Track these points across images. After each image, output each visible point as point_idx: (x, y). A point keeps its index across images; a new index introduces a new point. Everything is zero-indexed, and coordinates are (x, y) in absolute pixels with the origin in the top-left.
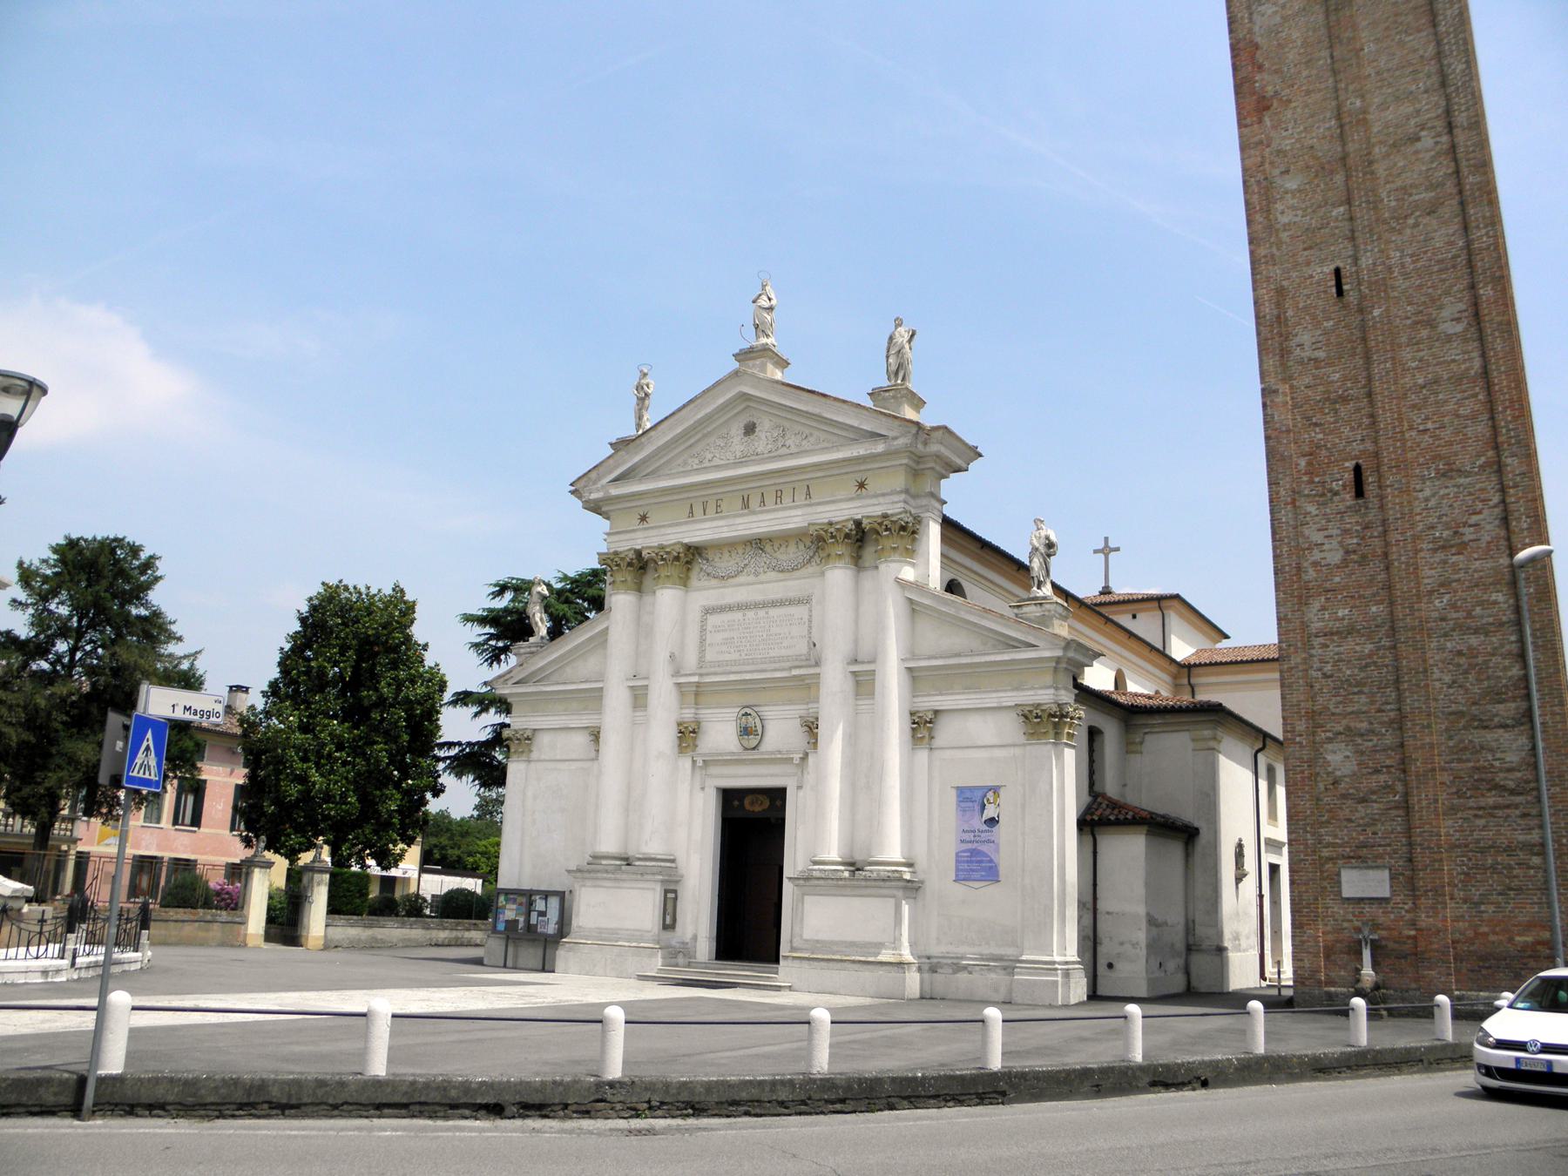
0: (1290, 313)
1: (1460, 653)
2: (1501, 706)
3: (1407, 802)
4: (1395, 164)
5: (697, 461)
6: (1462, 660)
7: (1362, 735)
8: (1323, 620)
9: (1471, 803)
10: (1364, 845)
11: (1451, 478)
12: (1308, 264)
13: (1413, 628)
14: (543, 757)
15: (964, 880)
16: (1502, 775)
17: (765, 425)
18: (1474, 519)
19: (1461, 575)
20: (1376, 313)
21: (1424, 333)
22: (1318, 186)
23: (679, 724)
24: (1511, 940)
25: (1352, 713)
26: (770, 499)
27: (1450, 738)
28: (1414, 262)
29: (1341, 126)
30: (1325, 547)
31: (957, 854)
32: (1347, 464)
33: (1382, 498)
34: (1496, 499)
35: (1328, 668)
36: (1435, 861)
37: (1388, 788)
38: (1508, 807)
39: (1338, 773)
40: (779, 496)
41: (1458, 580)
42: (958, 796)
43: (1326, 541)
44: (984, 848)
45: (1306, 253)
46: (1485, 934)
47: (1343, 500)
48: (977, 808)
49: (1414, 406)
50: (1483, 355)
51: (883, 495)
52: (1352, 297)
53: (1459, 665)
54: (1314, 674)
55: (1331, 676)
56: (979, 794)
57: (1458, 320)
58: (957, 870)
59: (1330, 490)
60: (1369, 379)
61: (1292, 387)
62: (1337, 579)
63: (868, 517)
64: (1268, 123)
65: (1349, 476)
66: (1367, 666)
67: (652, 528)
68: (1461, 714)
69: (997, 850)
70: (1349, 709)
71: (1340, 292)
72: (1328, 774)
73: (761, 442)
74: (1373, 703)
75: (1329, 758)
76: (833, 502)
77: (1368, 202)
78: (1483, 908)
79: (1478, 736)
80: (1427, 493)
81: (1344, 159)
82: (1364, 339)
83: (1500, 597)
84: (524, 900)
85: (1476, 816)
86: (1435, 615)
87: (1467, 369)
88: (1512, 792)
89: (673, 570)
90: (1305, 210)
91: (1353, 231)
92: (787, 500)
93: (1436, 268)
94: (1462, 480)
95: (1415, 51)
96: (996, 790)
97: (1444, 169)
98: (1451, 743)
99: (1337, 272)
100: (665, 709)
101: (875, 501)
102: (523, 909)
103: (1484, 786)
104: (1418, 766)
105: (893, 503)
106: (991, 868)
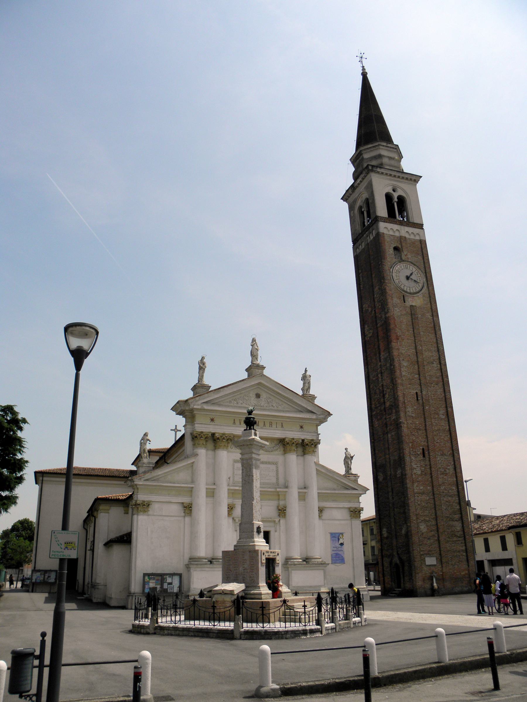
0: (406, 401)
1: (447, 501)
2: (456, 516)
3: (439, 539)
4: (428, 368)
5: (236, 402)
6: (448, 503)
7: (427, 521)
8: (417, 489)
9: (451, 540)
10: (430, 551)
11: (443, 456)
12: (410, 389)
13: (438, 494)
14: (155, 514)
15: (334, 563)
16: (457, 533)
17: (264, 395)
18: (448, 467)
19: (446, 481)
20: (427, 408)
21: (437, 416)
22: (411, 367)
23: (228, 505)
24: (460, 574)
25: (425, 515)
26: (267, 424)
27: (446, 523)
28: (434, 396)
29: (417, 352)
30: (417, 469)
31: (332, 555)
32: (421, 447)
33: (430, 458)
34: (453, 463)
35: (419, 502)
36: (446, 555)
37: (434, 536)
38: (458, 541)
39: (423, 531)
40: (271, 424)
41: (446, 483)
42: (331, 536)
43: (417, 467)
44: (339, 553)
45: (409, 385)
46: (456, 573)
47: (420, 457)
48: (337, 539)
49: (435, 435)
50: (449, 426)
51: (310, 432)
52: (420, 401)
53: (447, 505)
54: (416, 504)
55: (420, 505)
56: (337, 535)
57: (443, 415)
58: (332, 560)
59: (417, 454)
60: (425, 425)
61: (407, 423)
62: (420, 479)
63: (307, 439)
64: (399, 344)
65: (421, 451)
66: (428, 503)
67: (218, 425)
68: (448, 517)
69: (344, 553)
70: (425, 514)
71: (417, 399)
72: (421, 531)
73: (263, 401)
74: (429, 513)
75: (421, 527)
76: (292, 431)
77: (424, 377)
78: (455, 566)
79: (451, 523)
80: (439, 459)
81: (418, 362)
82: (424, 414)
83: (454, 488)
84: (160, 578)
85: (452, 543)
86: (441, 491)
87: (446, 428)
88: (459, 537)
90: (408, 373)
91: (420, 383)
92: (274, 426)
93: (438, 400)
94: (445, 457)
95: (432, 339)
96: (342, 534)
97: (439, 374)
98: (447, 524)
99: (417, 393)
101: (306, 434)
102: (159, 582)
103: (453, 535)
104: (441, 530)
105: (313, 436)
106: (342, 559)
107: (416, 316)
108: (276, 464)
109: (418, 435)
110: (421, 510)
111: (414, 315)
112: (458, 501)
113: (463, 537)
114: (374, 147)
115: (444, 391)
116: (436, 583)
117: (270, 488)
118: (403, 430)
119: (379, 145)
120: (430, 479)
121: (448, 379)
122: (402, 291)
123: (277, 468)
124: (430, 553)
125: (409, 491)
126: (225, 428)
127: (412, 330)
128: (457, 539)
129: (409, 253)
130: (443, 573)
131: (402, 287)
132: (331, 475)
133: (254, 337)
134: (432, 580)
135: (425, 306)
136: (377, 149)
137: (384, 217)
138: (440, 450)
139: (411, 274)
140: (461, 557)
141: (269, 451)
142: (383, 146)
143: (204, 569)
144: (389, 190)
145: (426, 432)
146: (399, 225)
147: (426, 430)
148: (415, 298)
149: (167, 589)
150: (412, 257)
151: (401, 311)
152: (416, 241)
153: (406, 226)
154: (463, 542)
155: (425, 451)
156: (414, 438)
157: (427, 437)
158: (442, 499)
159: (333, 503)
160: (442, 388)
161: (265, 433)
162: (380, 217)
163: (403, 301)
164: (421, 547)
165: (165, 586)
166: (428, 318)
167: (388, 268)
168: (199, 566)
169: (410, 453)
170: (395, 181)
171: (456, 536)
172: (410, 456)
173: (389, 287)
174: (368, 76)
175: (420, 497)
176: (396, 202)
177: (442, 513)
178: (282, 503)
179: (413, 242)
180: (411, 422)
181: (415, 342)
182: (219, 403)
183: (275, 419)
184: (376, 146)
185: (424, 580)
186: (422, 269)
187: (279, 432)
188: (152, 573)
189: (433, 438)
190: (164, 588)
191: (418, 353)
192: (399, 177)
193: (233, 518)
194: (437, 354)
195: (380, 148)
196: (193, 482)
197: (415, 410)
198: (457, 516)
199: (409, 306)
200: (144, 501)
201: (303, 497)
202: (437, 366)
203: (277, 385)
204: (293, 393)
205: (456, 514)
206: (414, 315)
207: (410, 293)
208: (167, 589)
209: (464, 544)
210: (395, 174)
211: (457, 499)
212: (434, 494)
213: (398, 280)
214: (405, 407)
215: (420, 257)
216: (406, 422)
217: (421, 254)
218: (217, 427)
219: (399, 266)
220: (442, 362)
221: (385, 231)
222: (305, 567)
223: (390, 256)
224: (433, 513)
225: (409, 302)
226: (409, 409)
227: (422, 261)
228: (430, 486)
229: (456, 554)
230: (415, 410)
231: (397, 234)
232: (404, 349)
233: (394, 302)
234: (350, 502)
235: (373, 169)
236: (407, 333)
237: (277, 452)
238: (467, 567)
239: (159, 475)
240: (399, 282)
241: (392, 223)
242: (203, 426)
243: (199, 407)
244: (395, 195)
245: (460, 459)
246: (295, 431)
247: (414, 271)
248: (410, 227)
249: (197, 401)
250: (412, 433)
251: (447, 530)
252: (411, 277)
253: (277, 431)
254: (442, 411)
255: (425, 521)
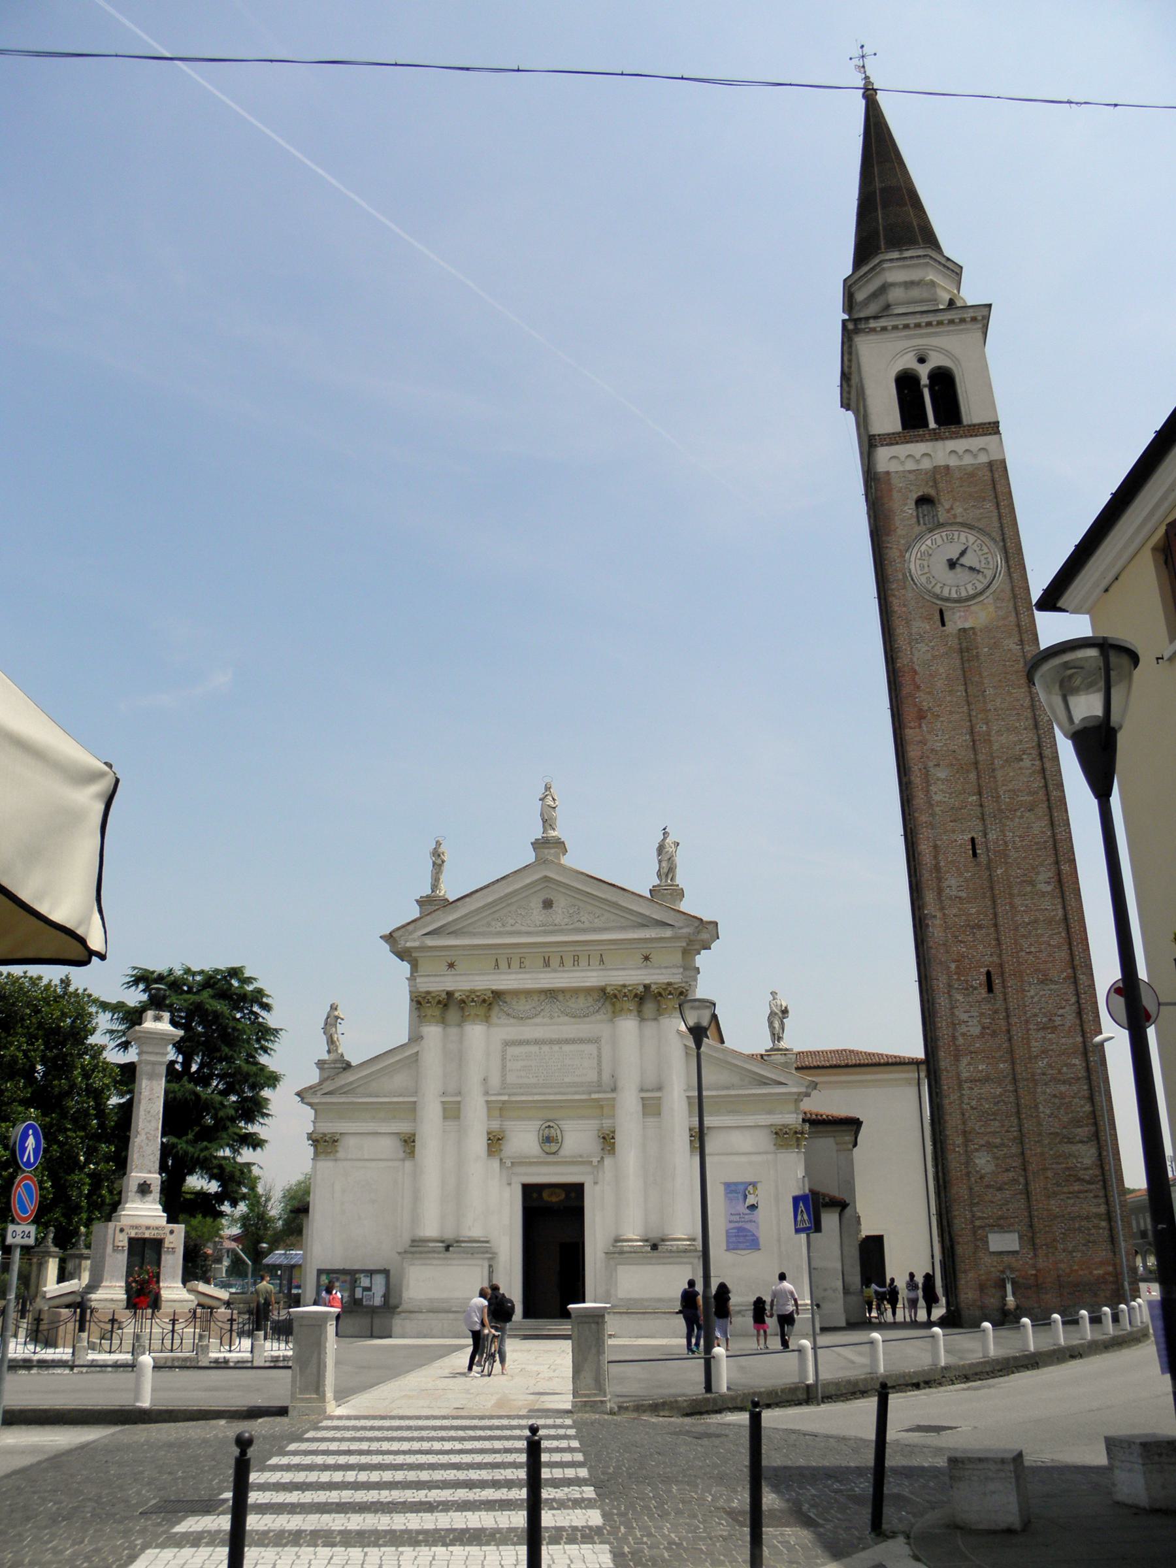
0: (942, 864)
1: (1055, 1096)
2: (1079, 1130)
3: (1027, 1189)
4: (1008, 774)
5: (500, 924)
6: (1057, 1101)
7: (997, 1147)
8: (969, 1071)
9: (1065, 1189)
10: (1001, 1218)
11: (1047, 985)
12: (954, 831)
13: (1027, 1080)
14: (349, 1157)
15: (734, 1249)
16: (1082, 1172)
17: (561, 902)
18: (1061, 1012)
19: (1054, 1046)
20: (999, 872)
21: (1029, 889)
22: (959, 779)
23: (488, 1133)
24: (1091, 1273)
25: (990, 1133)
26: (568, 962)
27: (1051, 1150)
28: (1021, 841)
29: (974, 741)
30: (969, 1024)
31: (727, 1232)
32: (982, 970)
33: (1005, 994)
34: (1073, 1000)
35: (974, 1103)
36: (1045, 1226)
37: (1015, 1181)
38: (1086, 1191)
39: (983, 1171)
40: (576, 960)
41: (1052, 1050)
42: (725, 1189)
43: (970, 1020)
44: (748, 1226)
45: (952, 824)
46: (1077, 1271)
47: (980, 993)
48: (741, 1197)
49: (1023, 936)
50: (1064, 908)
51: (666, 968)
52: (983, 859)
53: (1054, 1103)
54: (965, 1106)
55: (976, 1109)
56: (742, 1187)
57: (1048, 883)
58: (728, 1242)
59: (972, 986)
60: (995, 915)
61: (944, 914)
62: (978, 1045)
63: (655, 983)
64: (925, 729)
65: (983, 978)
66: (998, 1102)
67: (460, 975)
68: (1057, 1134)
69: (758, 1227)
70: (989, 1130)
71: (975, 855)
72: (977, 1172)
73: (559, 914)
74: (1003, 1126)
75: (977, 1161)
76: (624, 969)
77: (993, 797)
78: (1074, 1254)
79: (1067, 1148)
80: (1032, 993)
81: (976, 763)
82: (992, 888)
83: (1077, 1062)
84: (348, 1278)
85: (1068, 1198)
86: (1039, 1071)
87: (1054, 916)
88: (1089, 1183)
89: (481, 1011)
90: (951, 794)
91: (983, 814)
92: (583, 962)
93: (1034, 847)
94: (1053, 987)
95: (1018, 700)
96: (754, 1184)
97: (1038, 783)
98: (1051, 1153)
99: (973, 839)
100: (477, 1124)
101: (658, 971)
102: (347, 1286)
103: (1072, 1179)
104: (1033, 1167)
105: (674, 974)
106: (753, 1240)
107: (974, 652)
108: (596, 1041)
109: (974, 941)
110: (981, 1121)
111: (968, 650)
112: (1086, 1093)
113: (1101, 1183)
114: (873, 269)
115: (1052, 824)
116: (1014, 1294)
117: (576, 1093)
118: (930, 935)
119: (880, 262)
120: (1006, 1045)
121: (1063, 791)
122: (935, 601)
123: (599, 1049)
124: (1002, 1222)
125: (943, 1077)
126: (477, 978)
127: (962, 688)
128: (1082, 1187)
129: (958, 504)
130: (1037, 1270)
131: (937, 590)
132: (721, 1056)
133: (548, 780)
134: (1005, 1287)
135: (1001, 623)
136: (878, 273)
137: (889, 434)
138: (1037, 970)
139: (963, 553)
140: (1093, 1231)
141: (580, 1017)
142: (891, 260)
143: (429, 1262)
144: (908, 362)
145: (997, 931)
146: (931, 440)
147: (996, 925)
148: (973, 608)
149: (361, 1300)
150: (966, 510)
151: (933, 649)
152: (978, 467)
153: (951, 438)
154: (1101, 1194)
155: (994, 977)
156: (964, 950)
157: (999, 944)
158: (1039, 1090)
159: (731, 1118)
160: (1048, 817)
161: (562, 980)
162: (879, 435)
163: (939, 623)
164: (974, 1209)
165: (358, 1294)
166: (1010, 650)
167: (898, 554)
168: (418, 1256)
169: (950, 986)
170: (922, 336)
171: (1079, 1179)
172: (949, 993)
173: (899, 598)
174: (881, 98)
175: (976, 1091)
176: (925, 386)
177: (1039, 1124)
178: (607, 1123)
179: (970, 475)
180: (955, 911)
181: (970, 716)
182: (465, 930)
183: (585, 948)
184: (875, 266)
185: (982, 1288)
186: (994, 534)
187: (594, 974)
188: (344, 1269)
189: (1016, 943)
190: (356, 1297)
191: (978, 743)
192: (929, 324)
193: (501, 1160)
194: (1031, 735)
195: (883, 269)
196: (415, 1093)
197: (966, 880)
198: (1084, 1132)
199: (955, 632)
200: (325, 1135)
201: (652, 1107)
202: (1033, 765)
203: (580, 876)
204: (614, 889)
205: (1081, 1127)
206: (968, 650)
207: (959, 601)
208: (361, 1300)
209: (1102, 1200)
210: (917, 321)
211: (1085, 1087)
212: (1015, 1080)
213: (925, 576)
214: (939, 880)
215: (989, 505)
216: (939, 915)
217: (993, 496)
218: (458, 978)
219: (929, 542)
220: (1047, 752)
221: (893, 467)
222: (644, 1257)
223: (906, 522)
224: (1011, 1127)
225: (955, 623)
226: (952, 882)
227: (995, 514)
228: (1005, 1061)
229: (1077, 1226)
230: (966, 880)
231: (926, 464)
232: (939, 738)
233: (914, 630)
234: (770, 1112)
235: (859, 327)
236: (948, 698)
237: (599, 1017)
238: (1110, 1255)
239: (351, 1083)
240: (928, 578)
241: (912, 442)
242: (432, 979)
243: (416, 944)
244: (923, 372)
245: (1095, 989)
246: (632, 969)
247: (970, 544)
248: (961, 437)
249: (411, 933)
250: (956, 937)
251: (1054, 1166)
252: (963, 561)
253: (589, 974)
254: (1045, 875)
255: (989, 1145)
